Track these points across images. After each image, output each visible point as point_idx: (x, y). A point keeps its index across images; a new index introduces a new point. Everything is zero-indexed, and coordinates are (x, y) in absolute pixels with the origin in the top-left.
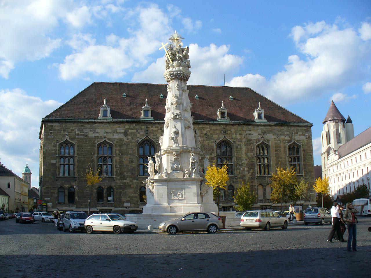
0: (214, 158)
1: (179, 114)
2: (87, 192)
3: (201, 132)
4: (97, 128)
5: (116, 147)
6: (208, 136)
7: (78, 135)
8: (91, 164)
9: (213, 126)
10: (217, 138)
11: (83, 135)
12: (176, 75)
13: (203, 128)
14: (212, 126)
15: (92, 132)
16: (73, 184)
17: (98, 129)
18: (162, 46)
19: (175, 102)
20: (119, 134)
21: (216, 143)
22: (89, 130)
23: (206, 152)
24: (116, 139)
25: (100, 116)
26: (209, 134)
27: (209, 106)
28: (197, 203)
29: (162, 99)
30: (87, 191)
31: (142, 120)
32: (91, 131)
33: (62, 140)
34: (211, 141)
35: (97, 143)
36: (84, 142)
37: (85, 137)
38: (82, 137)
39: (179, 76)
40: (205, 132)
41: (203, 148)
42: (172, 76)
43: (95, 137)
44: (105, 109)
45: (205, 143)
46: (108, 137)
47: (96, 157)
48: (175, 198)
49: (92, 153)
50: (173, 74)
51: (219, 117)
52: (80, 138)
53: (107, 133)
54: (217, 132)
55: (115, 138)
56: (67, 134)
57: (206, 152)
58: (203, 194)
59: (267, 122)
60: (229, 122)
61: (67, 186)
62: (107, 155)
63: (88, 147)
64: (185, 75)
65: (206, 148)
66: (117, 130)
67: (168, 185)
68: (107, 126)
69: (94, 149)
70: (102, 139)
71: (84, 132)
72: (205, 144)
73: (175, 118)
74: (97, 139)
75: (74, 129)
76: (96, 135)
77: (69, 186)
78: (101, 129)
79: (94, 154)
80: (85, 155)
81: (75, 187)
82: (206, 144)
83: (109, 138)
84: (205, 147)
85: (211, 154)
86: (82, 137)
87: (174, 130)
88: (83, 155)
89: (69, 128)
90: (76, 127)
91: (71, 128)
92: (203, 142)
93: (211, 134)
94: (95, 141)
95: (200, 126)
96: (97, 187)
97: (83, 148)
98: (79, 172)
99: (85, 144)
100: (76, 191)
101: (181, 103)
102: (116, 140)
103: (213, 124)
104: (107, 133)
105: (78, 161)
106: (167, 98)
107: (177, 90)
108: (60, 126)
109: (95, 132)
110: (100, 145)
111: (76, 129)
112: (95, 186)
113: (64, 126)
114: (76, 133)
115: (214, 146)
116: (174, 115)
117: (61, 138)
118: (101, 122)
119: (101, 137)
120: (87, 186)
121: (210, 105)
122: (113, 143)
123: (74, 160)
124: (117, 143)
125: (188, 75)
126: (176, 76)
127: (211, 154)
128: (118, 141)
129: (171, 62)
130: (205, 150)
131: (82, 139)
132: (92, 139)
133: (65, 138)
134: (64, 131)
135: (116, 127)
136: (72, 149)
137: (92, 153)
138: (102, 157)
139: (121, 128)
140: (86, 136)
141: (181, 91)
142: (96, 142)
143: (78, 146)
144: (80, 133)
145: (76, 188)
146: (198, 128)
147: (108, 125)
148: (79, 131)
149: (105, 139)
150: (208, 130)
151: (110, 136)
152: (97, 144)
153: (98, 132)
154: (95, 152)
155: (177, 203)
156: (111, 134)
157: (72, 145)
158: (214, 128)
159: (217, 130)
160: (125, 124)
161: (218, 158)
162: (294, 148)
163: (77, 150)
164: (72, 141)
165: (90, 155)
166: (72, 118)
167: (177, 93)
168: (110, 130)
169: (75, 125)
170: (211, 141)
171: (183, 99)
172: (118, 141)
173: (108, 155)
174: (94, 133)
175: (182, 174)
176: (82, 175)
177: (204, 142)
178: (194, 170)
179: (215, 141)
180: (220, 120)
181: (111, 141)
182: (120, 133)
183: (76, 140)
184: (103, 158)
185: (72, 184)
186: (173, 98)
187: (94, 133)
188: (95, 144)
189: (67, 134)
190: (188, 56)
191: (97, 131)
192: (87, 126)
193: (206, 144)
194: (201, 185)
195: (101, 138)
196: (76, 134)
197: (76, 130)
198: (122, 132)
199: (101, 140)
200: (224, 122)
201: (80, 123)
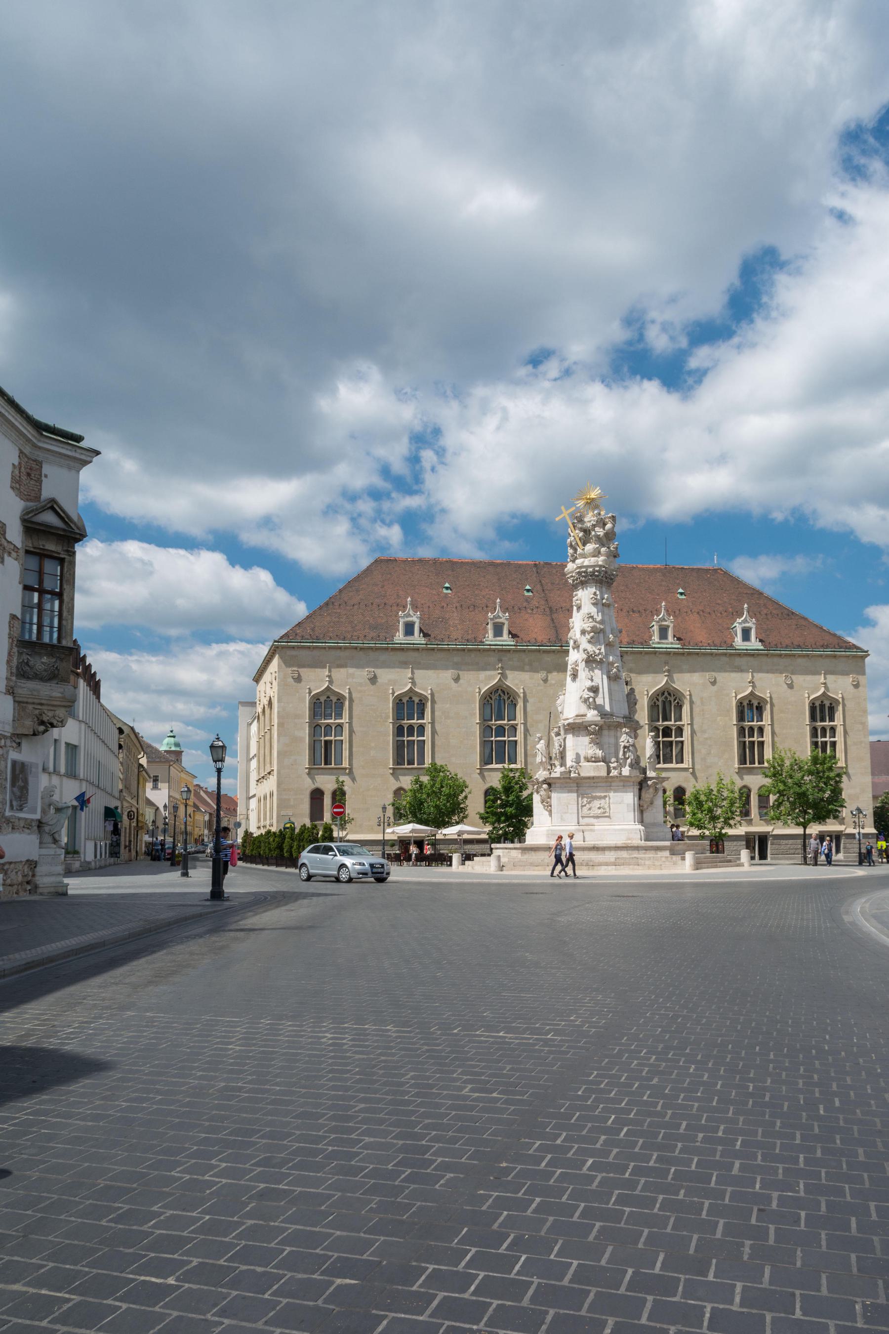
18: (562, 513)
25: (400, 637)
27: (633, 611)
29: (529, 597)
31: (490, 645)
39: (597, 576)
73: (591, 661)
87: (589, 684)
107: (593, 604)
141: (600, 606)
162: (822, 706)
166: (340, 639)
167: (594, 610)
178: (629, 761)
180: (659, 643)
186: (586, 619)
194: (640, 790)
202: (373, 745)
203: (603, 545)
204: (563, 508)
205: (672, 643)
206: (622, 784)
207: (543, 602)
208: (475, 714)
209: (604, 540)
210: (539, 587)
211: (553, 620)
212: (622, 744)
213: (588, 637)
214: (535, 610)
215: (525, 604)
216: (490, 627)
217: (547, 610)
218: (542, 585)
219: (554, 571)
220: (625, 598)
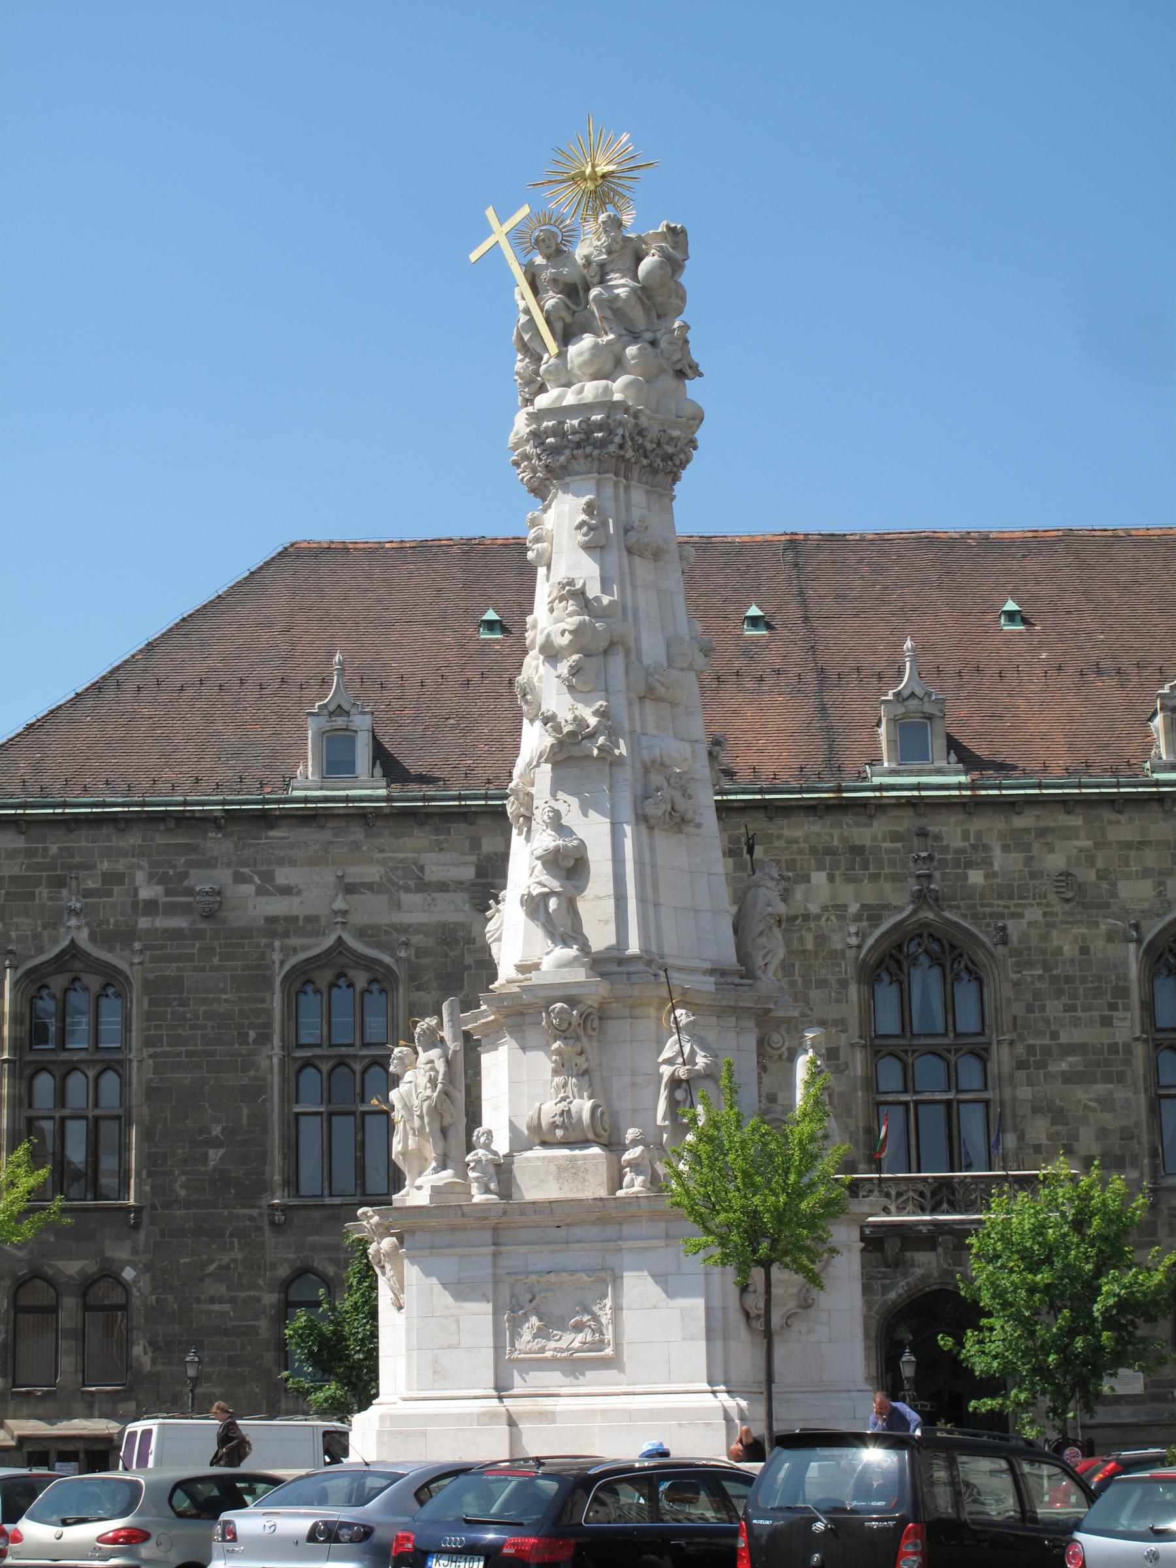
0: (1128, 1049)
1: (593, 721)
2: (216, 1307)
3: (1028, 861)
4: (281, 862)
5: (418, 988)
6: (1081, 888)
7: (151, 907)
8: (245, 1112)
9: (1114, 817)
10: (1146, 905)
11: (187, 909)
12: (576, 438)
13: (1042, 832)
14: (1108, 815)
15: (248, 889)
16: (119, 1252)
17: (292, 863)
18: (489, 232)
19: (568, 637)
20: (438, 895)
21: (1139, 941)
22: (229, 872)
23: (1069, 1008)
24: (419, 929)
26: (1088, 875)
27: (1099, 671)
28: (495, 1393)
29: (755, 641)
30: (212, 1300)
32: (239, 878)
33: (40, 950)
34: (1103, 927)
35: (281, 962)
36: (190, 958)
37: (203, 925)
38: (180, 922)
39: (603, 444)
40: (1055, 861)
41: (1040, 978)
42: (554, 451)
43: (271, 920)
44: (340, 722)
45: (1056, 943)
46: (358, 919)
47: (275, 1060)
48: (548, 1354)
49: (252, 1034)
50: (558, 431)
51: (1163, 750)
52: (166, 931)
53: (350, 889)
54: (1151, 859)
55: (410, 926)
56: (78, 905)
57: (1069, 1008)
61: (72, 1268)
62: (358, 1043)
63: (224, 991)
64: (654, 433)
65: (1068, 980)
66: (422, 869)
67: (495, 1256)
68: (356, 846)
69: (267, 1006)
70: (316, 933)
71: (190, 892)
72: (1059, 951)
74: (286, 935)
75: (121, 866)
76: (278, 906)
77: (92, 1266)
78: (313, 862)
79: (264, 1039)
80: (200, 1047)
81: (128, 1274)
82: (1069, 950)
83: (371, 927)
84: (1054, 972)
85: (1106, 1022)
86: (180, 922)
88: (183, 1049)
89: (91, 867)
90: (141, 855)
91: (106, 865)
92: (1045, 937)
93: (1103, 875)
94: (270, 945)
95: (1019, 822)
96: (283, 1272)
97: (183, 1003)
98: (153, 1164)
99: (203, 969)
100: (136, 1302)
101: (612, 644)
102: (417, 939)
103: (1113, 802)
104: (350, 889)
105: (151, 1093)
106: (531, 612)
107: (587, 547)
108: (30, 853)
109: (268, 886)
110: (301, 979)
111: (140, 867)
112: (273, 1267)
113: (54, 849)
114: (136, 895)
115: (1125, 964)
116: (557, 728)
117: (36, 936)
118: (311, 817)
119: (309, 919)
120: (212, 1268)
121: (1106, 664)
122: (398, 960)
123: (125, 1084)
124: (425, 961)
125: (676, 433)
126: (578, 445)
127: (1106, 1022)
128: (431, 943)
129: (553, 347)
130: (1059, 993)
131: (177, 934)
132: (246, 933)
133: (62, 930)
134: (58, 883)
135: (413, 845)
136: (110, 1005)
137: (252, 1034)
138: (321, 1057)
139: (448, 856)
140: (209, 916)
141: (615, 555)
142: (277, 957)
143: (150, 987)
144: (167, 894)
145: (135, 1281)
146: (1002, 836)
147: (357, 833)
148: (158, 883)
149: (339, 932)
150: (1081, 850)
151: (372, 910)
152: (287, 967)
153: (292, 882)
154: (268, 1025)
155: (563, 1391)
156: (384, 898)
157: (113, 979)
158: (1124, 828)
159: (1143, 844)
160: (482, 821)
161: (1157, 1046)
163: (148, 1017)
164: (111, 950)
165: (236, 1046)
166: (114, 793)
168: (373, 873)
169: (133, 839)
170: (1103, 927)
171: (635, 611)
172: (431, 943)
173: (365, 1045)
174: (260, 892)
175: (603, 1169)
176: (182, 1193)
177: (1054, 933)
179: (1137, 927)
181: (378, 945)
182: (443, 887)
183: (137, 946)
184: (325, 1067)
185: (108, 1254)
187: (260, 892)
188: (269, 967)
189: (78, 905)
190: (681, 295)
191: (283, 876)
192: (216, 844)
193: (1069, 950)
195: (309, 927)
196: (135, 905)
197: (140, 876)
198: (459, 885)
199: (312, 940)
201: (162, 827)
202: (216, 1130)
203: (635, 337)
206: (661, 1227)
209: (638, 315)
210: (794, 611)
211: (823, 708)
212: (666, 1071)
213: (564, 668)
214: (770, 681)
215: (738, 664)
217: (811, 677)
218: (804, 603)
219: (852, 559)
220: (1075, 633)
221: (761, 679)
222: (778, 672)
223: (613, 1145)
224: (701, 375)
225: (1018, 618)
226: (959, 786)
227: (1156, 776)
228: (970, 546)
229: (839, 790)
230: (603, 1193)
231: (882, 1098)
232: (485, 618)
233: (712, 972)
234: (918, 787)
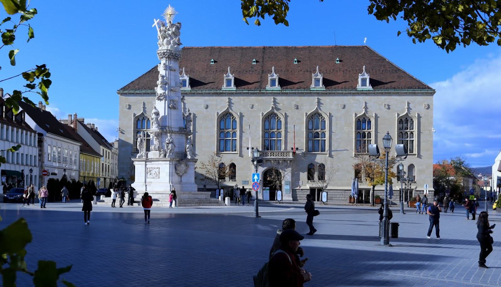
29: (254, 65)
50: (160, 52)
58: (181, 174)
59: (372, 89)
60: (323, 91)
64: (174, 53)
101: (166, 83)
129: (162, 41)
200: (317, 90)
204: (155, 20)
205: (321, 88)
207: (260, 68)
208: (215, 126)
215: (250, 69)
216: (225, 81)
218: (263, 59)
221: (253, 72)
222: (256, 70)
223: (160, 151)
224: (182, 44)
225: (297, 62)
226: (279, 90)
227: (311, 89)
228: (293, 49)
229: (260, 91)
230: (158, 157)
231: (265, 139)
232: (211, 61)
233: (179, 128)
234: (273, 90)
